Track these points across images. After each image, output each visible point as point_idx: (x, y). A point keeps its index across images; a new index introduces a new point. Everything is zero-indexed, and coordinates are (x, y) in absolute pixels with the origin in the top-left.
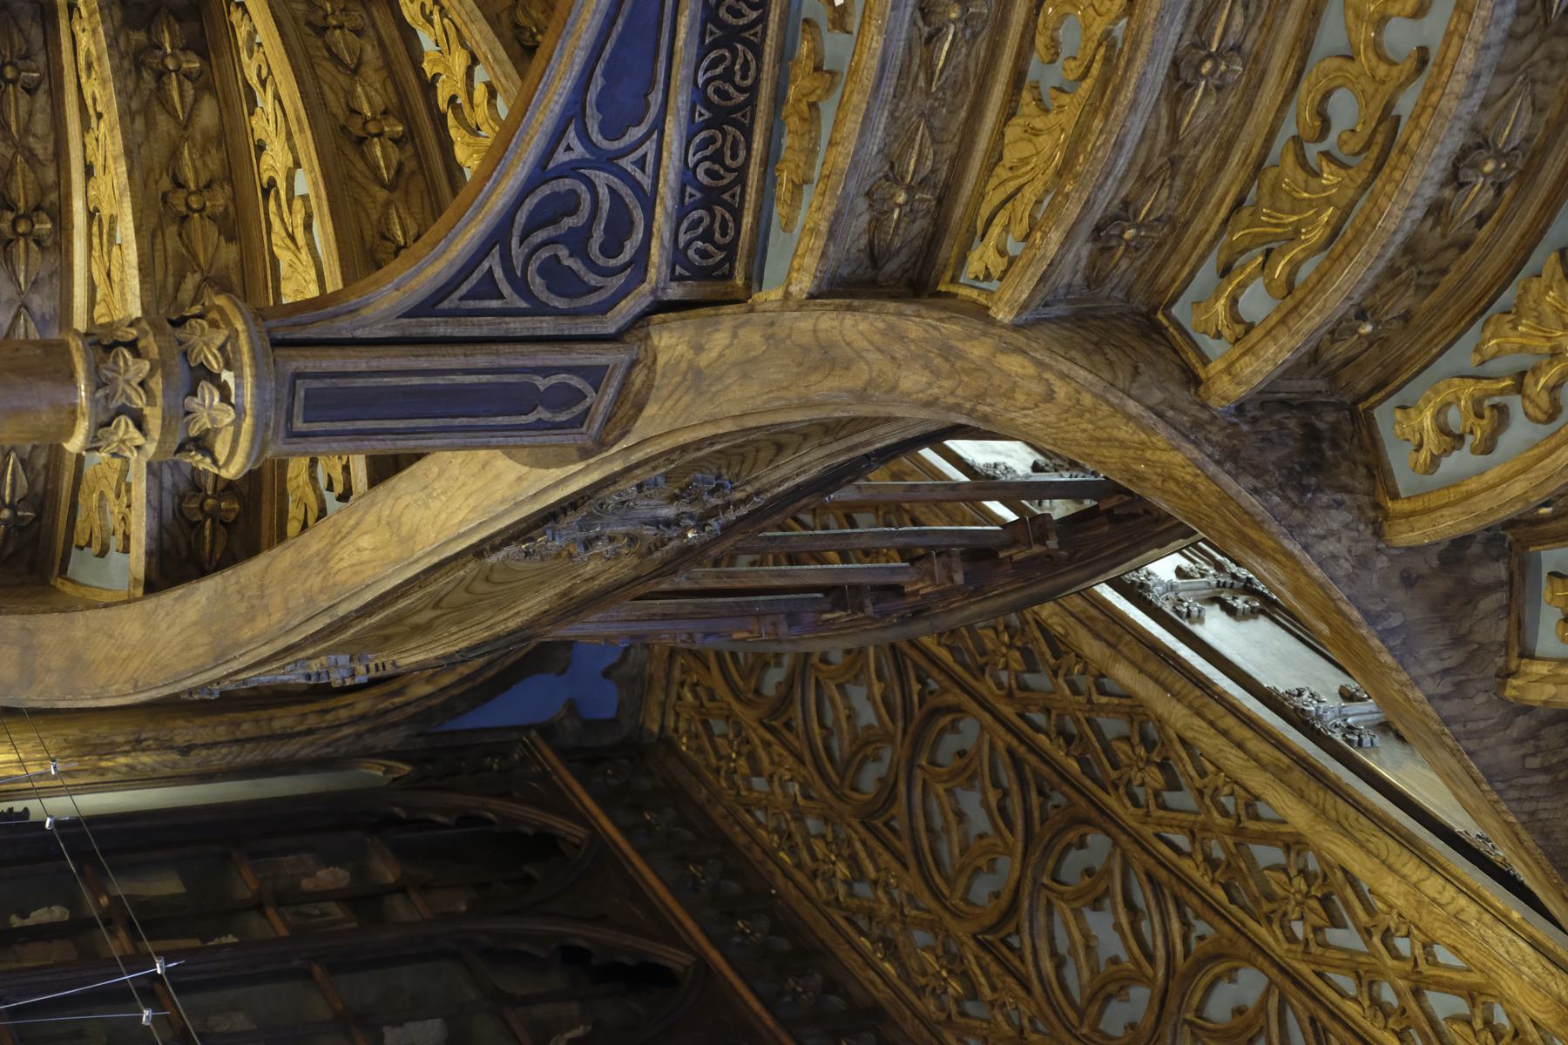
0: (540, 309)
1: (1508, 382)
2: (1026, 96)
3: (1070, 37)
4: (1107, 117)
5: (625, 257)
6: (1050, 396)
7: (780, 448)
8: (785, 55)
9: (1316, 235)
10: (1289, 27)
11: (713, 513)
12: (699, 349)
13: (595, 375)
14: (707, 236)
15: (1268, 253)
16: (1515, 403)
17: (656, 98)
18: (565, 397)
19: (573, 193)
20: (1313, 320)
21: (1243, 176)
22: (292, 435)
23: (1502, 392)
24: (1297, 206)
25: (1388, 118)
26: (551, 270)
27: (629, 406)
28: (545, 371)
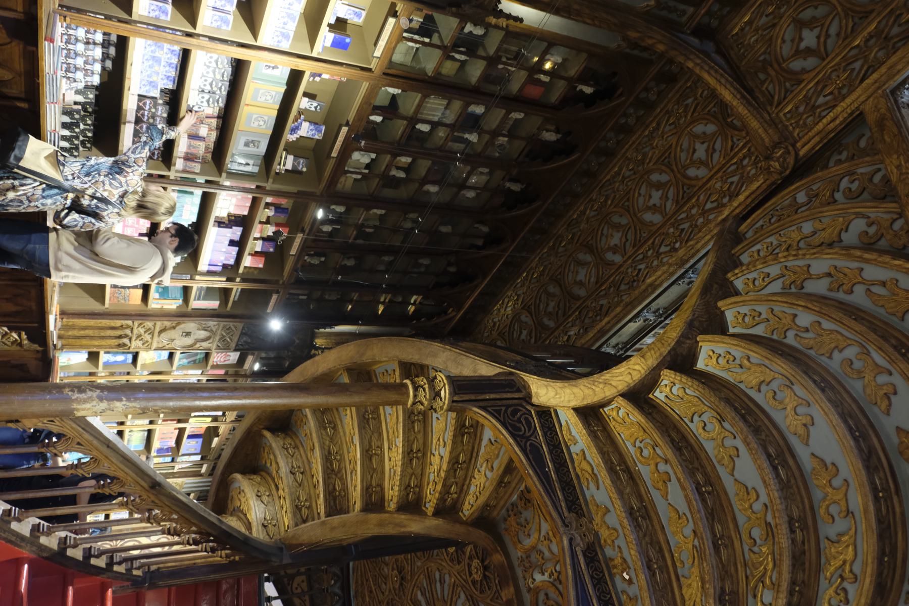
1: (839, 580)
2: (682, 579)
3: (684, 558)
4: (706, 561)
9: (770, 566)
10: (731, 526)
15: (762, 582)
20: (785, 586)
21: (743, 569)
23: (840, 584)
24: (761, 563)
25: (768, 524)
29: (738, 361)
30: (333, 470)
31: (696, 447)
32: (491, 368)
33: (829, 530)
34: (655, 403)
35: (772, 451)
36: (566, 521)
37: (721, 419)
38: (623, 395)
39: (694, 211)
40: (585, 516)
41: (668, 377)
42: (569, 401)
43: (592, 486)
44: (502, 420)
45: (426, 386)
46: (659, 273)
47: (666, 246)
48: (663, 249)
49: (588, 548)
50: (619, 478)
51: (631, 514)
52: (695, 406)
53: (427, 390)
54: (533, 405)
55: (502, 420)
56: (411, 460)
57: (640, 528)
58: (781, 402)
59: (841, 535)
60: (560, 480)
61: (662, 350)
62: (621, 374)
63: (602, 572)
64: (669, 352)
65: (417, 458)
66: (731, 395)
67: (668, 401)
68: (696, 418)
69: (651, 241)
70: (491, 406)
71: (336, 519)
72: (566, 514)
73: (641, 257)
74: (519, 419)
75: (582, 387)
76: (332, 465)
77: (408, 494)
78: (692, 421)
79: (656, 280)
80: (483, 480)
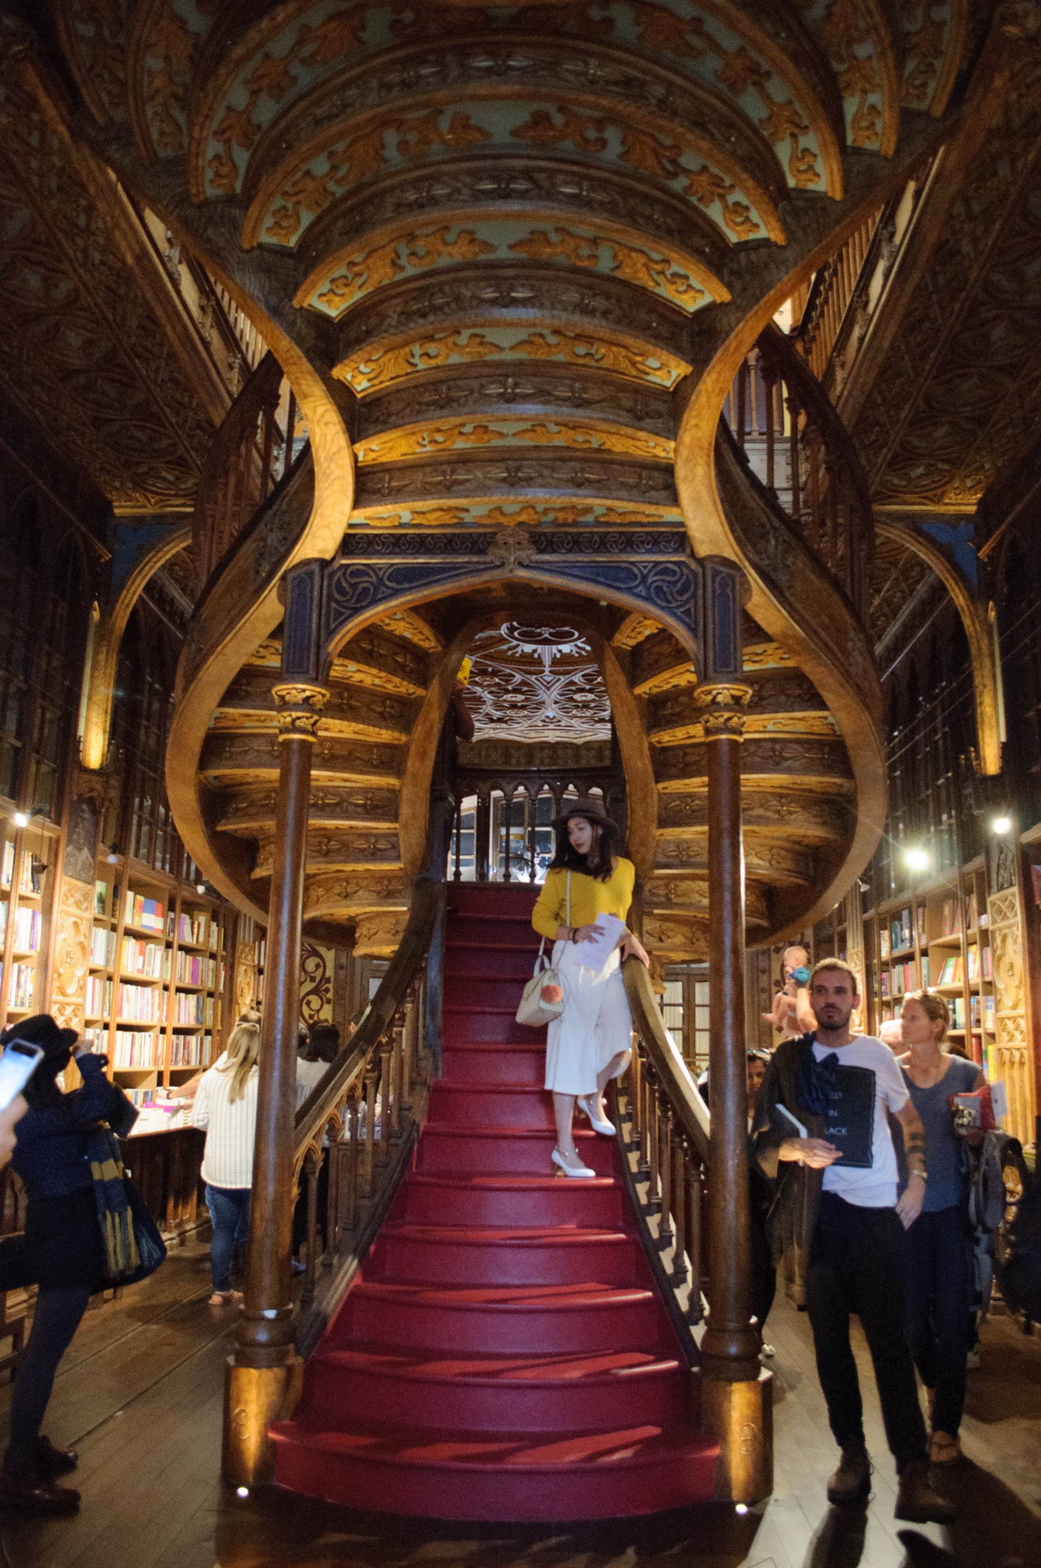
0: (694, 595)
5: (676, 569)
6: (696, 426)
7: (745, 507)
8: (608, 524)
11: (772, 526)
12: (703, 542)
13: (716, 574)
14: (669, 542)
16: (668, 273)
17: (624, 565)
18: (723, 586)
19: (656, 587)
22: (735, 671)
26: (681, 593)
27: (725, 562)
28: (714, 591)
29: (350, 276)
30: (337, 804)
31: (454, 374)
32: (267, 602)
33: (604, 264)
34: (372, 397)
35: (490, 294)
36: (498, 563)
37: (430, 338)
38: (353, 440)
39: (34, 164)
40: (495, 534)
41: (342, 372)
42: (342, 514)
43: (462, 515)
44: (348, 612)
45: (294, 714)
46: (123, 245)
47: (77, 217)
48: (82, 221)
49: (535, 543)
50: (462, 482)
51: (512, 485)
52: (396, 358)
53: (299, 714)
54: (333, 559)
55: (348, 612)
56: (351, 707)
57: (532, 479)
58: (429, 253)
59: (615, 257)
60: (443, 551)
61: (304, 368)
62: (324, 436)
63: (566, 534)
64: (310, 361)
65: (350, 698)
66: (394, 302)
67: (376, 382)
68: (416, 360)
69: (60, 235)
70: (328, 622)
71: (405, 810)
72: (488, 559)
73: (80, 255)
74: (352, 586)
75: (329, 492)
76: (329, 805)
77: (392, 717)
78: (415, 365)
79: (133, 251)
80: (402, 624)
